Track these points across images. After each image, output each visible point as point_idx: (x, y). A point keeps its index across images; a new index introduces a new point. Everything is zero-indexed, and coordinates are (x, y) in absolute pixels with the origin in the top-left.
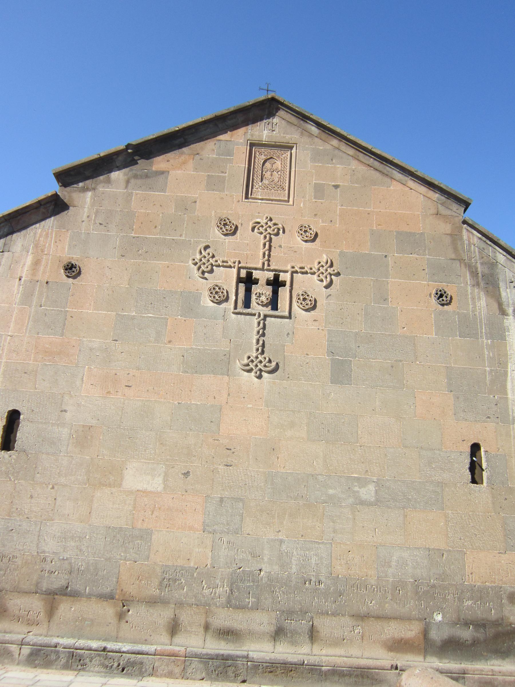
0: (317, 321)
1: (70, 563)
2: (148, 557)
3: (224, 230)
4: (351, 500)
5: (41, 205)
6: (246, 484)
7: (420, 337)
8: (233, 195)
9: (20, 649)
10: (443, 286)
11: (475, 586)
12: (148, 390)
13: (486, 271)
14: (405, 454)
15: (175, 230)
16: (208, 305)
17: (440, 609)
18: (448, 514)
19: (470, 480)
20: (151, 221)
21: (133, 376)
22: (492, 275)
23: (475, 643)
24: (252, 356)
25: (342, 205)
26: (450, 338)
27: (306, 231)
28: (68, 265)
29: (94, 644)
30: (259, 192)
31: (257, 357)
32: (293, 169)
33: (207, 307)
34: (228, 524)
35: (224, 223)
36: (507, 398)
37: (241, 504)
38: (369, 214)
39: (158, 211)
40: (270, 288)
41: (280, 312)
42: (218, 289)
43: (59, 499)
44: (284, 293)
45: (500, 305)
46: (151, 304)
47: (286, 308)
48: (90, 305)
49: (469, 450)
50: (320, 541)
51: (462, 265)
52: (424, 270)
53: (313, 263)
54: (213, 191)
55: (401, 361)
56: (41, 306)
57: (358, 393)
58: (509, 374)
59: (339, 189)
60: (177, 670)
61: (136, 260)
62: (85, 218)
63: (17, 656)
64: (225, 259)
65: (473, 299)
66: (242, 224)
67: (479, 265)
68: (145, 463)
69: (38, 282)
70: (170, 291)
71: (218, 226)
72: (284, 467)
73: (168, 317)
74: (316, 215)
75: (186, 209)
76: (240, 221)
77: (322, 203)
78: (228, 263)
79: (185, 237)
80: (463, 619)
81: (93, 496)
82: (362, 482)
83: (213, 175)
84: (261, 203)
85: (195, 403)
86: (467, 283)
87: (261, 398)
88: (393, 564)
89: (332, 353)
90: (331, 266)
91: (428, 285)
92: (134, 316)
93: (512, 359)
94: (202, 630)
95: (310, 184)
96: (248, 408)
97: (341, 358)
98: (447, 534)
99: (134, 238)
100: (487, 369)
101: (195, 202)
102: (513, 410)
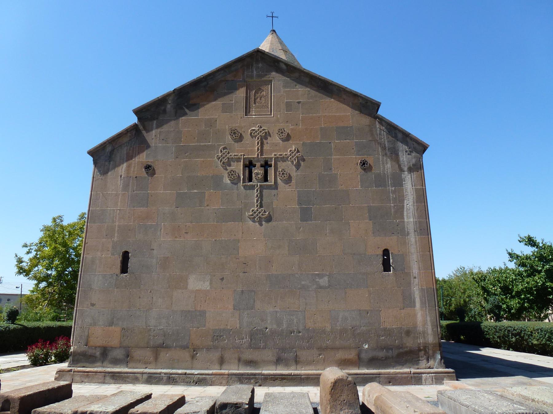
1: (164, 331)
2: (205, 326)
3: (234, 136)
4: (315, 286)
5: (128, 132)
6: (255, 282)
9: (142, 376)
10: (365, 157)
11: (387, 328)
13: (391, 146)
14: (345, 259)
17: (366, 342)
18: (370, 290)
19: (383, 270)
22: (394, 148)
23: (387, 358)
26: (370, 189)
27: (282, 133)
28: (146, 166)
29: (180, 371)
31: (257, 210)
32: (273, 94)
33: (227, 183)
34: (247, 305)
36: (404, 221)
37: (253, 293)
41: (269, 183)
43: (154, 298)
44: (271, 171)
45: (399, 166)
48: (161, 188)
49: (382, 253)
50: (298, 310)
51: (376, 143)
52: (353, 149)
53: (287, 152)
54: (226, 113)
55: (340, 205)
56: (134, 191)
58: (405, 207)
60: (224, 382)
62: (153, 137)
63: (141, 380)
64: (236, 154)
65: (383, 163)
66: (244, 132)
67: (386, 143)
68: (199, 274)
69: (131, 177)
72: (276, 271)
74: (287, 122)
78: (237, 156)
80: (380, 346)
81: (172, 295)
82: (320, 276)
84: (255, 117)
85: (224, 239)
86: (379, 154)
88: (340, 319)
89: (300, 204)
90: (298, 151)
91: (356, 158)
93: (407, 198)
94: (236, 361)
97: (306, 206)
98: (370, 301)
100: (392, 205)
101: (216, 121)
102: (407, 227)
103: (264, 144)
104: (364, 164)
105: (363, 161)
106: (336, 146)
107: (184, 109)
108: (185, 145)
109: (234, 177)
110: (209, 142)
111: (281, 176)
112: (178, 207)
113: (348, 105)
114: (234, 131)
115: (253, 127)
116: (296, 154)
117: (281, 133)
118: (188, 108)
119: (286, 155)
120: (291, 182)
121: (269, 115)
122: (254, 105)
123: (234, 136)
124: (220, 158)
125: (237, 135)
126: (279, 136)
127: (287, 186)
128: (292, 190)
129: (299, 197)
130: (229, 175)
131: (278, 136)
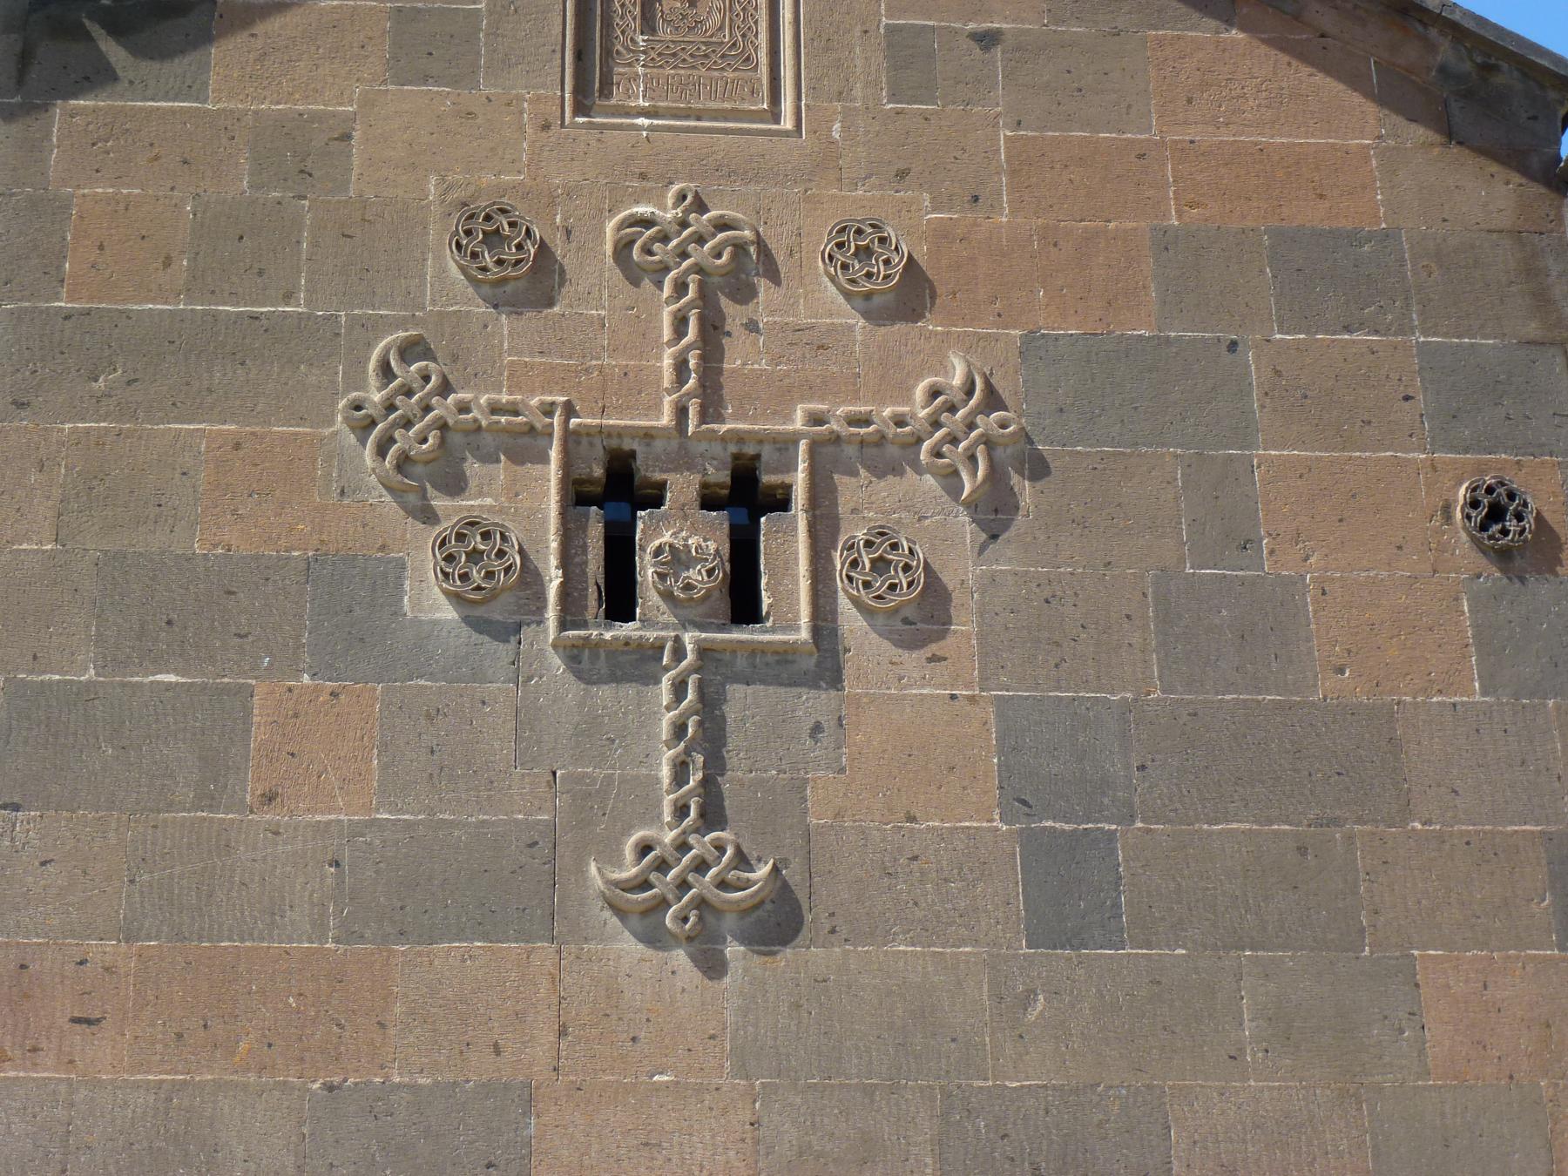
0: (945, 659)
3: (488, 260)
7: (1415, 705)
8: (520, 98)
10: (1500, 464)
12: (180, 1036)
15: (260, 273)
16: (437, 615)
20: (144, 233)
21: (107, 969)
24: (660, 843)
25: (1019, 123)
26: (1551, 703)
27: (864, 253)
30: (636, 76)
31: (683, 847)
33: (435, 623)
35: (484, 232)
38: (1141, 156)
39: (172, 189)
40: (719, 520)
41: (773, 630)
42: (478, 538)
46: (169, 623)
47: (799, 610)
52: (1407, 398)
53: (906, 396)
54: (425, 83)
55: (1335, 822)
57: (1159, 983)
59: (999, 48)
61: (83, 420)
64: (505, 398)
66: (568, 232)
70: (257, 558)
71: (459, 246)
73: (254, 682)
74: (902, 174)
75: (302, 171)
76: (558, 220)
77: (926, 119)
78: (517, 414)
79: (308, 303)
83: (419, 11)
84: (651, 128)
87: (712, 1037)
89: (1024, 803)
90: (993, 401)
91: (1434, 469)
92: (89, 682)
95: (866, 32)
96: (658, 1088)
97: (1067, 827)
99: (67, 318)
101: (346, 137)
103: (729, 334)
104: (1496, 514)
105: (1490, 490)
106: (1278, 373)
107: (88, 37)
108: (88, 313)
109: (490, 575)
110: (288, 297)
111: (867, 585)
112: (16, 800)
113: (1355, 81)
114: (488, 218)
115: (637, 202)
116: (979, 419)
117: (856, 254)
118: (118, 28)
119: (900, 422)
120: (941, 635)
121: (762, 121)
122: (640, 38)
123: (488, 260)
124: (374, 423)
125: (510, 254)
126: (841, 278)
127: (912, 660)
128: (953, 697)
129: (1009, 746)
130: (450, 558)
131: (833, 280)
